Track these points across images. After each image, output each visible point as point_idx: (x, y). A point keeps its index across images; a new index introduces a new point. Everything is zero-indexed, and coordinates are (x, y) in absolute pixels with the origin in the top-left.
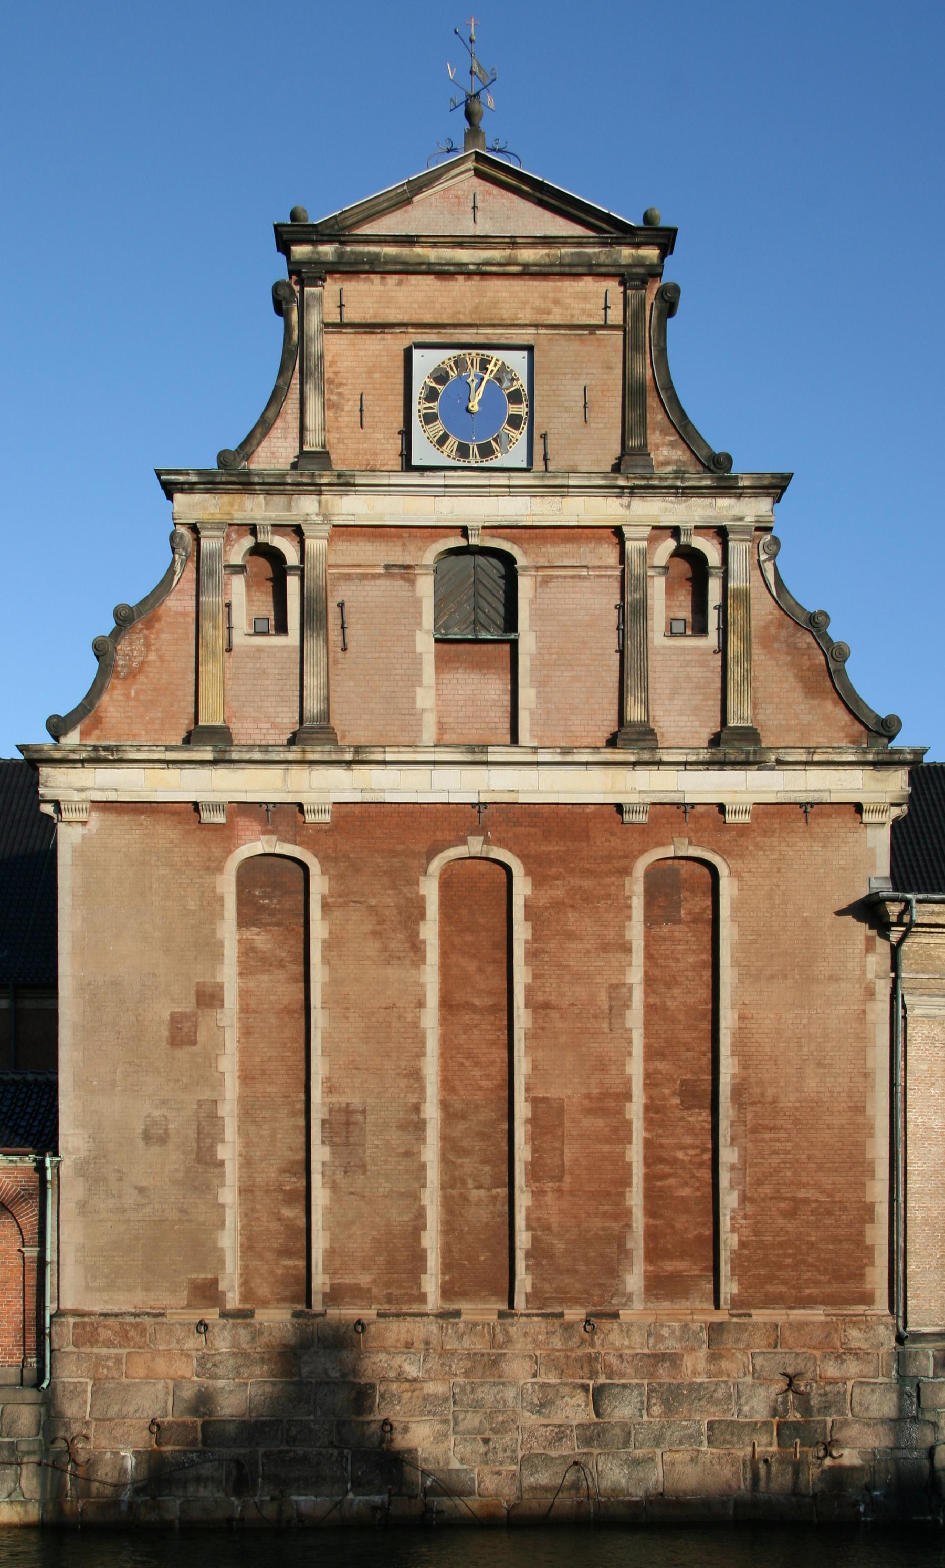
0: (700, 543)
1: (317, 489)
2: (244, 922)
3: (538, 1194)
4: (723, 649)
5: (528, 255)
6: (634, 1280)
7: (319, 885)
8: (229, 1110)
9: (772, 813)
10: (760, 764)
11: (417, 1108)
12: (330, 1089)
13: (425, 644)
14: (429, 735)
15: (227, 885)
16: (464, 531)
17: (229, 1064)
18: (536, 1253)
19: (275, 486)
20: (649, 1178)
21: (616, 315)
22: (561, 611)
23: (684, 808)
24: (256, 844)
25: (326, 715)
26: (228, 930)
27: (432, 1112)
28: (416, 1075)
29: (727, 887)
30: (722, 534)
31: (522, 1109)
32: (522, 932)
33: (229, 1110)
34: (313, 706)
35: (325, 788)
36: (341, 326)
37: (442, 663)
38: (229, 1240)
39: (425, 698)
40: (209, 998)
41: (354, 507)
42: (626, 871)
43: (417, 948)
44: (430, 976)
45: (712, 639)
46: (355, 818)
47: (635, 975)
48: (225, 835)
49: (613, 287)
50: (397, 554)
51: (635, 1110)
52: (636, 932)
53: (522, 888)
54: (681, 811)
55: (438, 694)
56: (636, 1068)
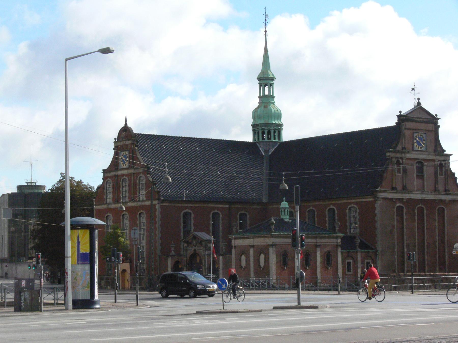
0: (443, 162)
1: (404, 153)
2: (397, 215)
3: (428, 256)
4: (445, 178)
5: (425, 120)
6: (437, 269)
7: (405, 210)
8: (396, 244)
9: (450, 201)
10: (450, 194)
11: (415, 243)
12: (406, 241)
13: (415, 176)
14: (416, 189)
15: (395, 210)
16: (418, 159)
17: (396, 237)
18: (428, 264)
19: (398, 152)
20: (439, 253)
21: (434, 129)
22: (428, 171)
23: (441, 200)
24: (398, 205)
25: (406, 186)
26: (395, 217)
27: (417, 244)
28: (415, 238)
29: (446, 212)
30: (444, 161)
31: (426, 244)
32: (425, 218)
33: (396, 244)
34: (404, 184)
35: (406, 196)
36: (406, 129)
37: (417, 178)
38: (396, 263)
39: (415, 183)
40: (394, 227)
41: (408, 156)
42: (436, 209)
43: (415, 219)
44: (416, 224)
45: (444, 176)
46: (409, 200)
47: (437, 225)
48: (396, 203)
49: (433, 125)
50: (412, 162)
51: (437, 243)
52: (437, 218)
53: (425, 212)
54: (441, 201)
55: (416, 182)
56: (437, 238)
